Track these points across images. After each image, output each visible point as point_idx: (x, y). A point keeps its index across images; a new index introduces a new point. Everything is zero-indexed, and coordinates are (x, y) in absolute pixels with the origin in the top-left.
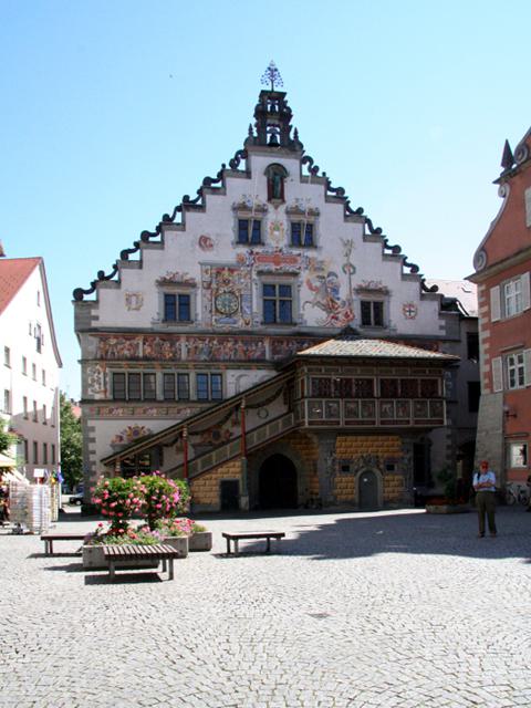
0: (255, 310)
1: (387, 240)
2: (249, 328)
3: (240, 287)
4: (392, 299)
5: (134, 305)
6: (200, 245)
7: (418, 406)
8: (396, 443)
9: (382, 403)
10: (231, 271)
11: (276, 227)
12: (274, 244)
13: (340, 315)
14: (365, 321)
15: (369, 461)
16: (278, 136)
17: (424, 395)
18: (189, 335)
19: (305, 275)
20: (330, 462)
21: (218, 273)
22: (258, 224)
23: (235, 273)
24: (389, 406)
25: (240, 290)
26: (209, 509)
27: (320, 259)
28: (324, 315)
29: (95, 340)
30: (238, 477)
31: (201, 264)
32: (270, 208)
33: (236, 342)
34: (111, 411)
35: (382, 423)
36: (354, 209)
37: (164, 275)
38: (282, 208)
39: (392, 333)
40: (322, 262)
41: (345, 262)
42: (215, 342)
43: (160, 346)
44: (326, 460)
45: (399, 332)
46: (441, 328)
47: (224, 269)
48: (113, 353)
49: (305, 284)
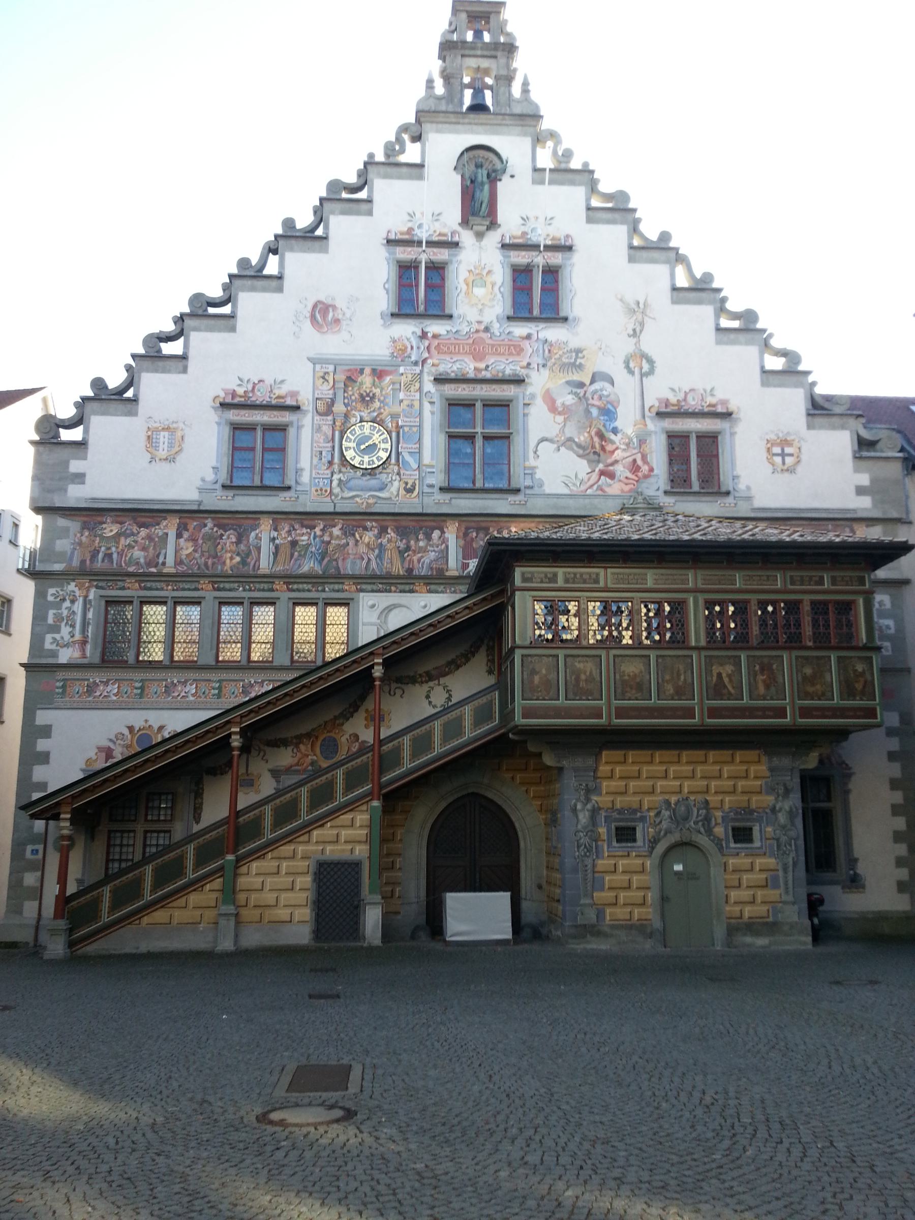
0: (427, 459)
1: (724, 300)
3: (396, 409)
4: (740, 428)
5: (162, 453)
6: (313, 317)
8: (753, 768)
9: (710, 660)
10: (378, 374)
11: (479, 277)
15: (686, 819)
16: (488, 94)
17: (822, 641)
18: (278, 516)
20: (584, 818)
21: (350, 380)
22: (437, 270)
23: (388, 379)
24: (729, 669)
25: (394, 416)
27: (574, 343)
28: (582, 467)
29: (72, 525)
30: (361, 851)
31: (314, 361)
32: (466, 237)
33: (383, 531)
34: (91, 689)
35: (714, 712)
36: (653, 236)
37: (233, 385)
38: (493, 239)
39: (743, 510)
40: (578, 351)
42: (336, 531)
43: (214, 540)
44: (574, 810)
45: (757, 503)
46: (860, 491)
47: (361, 371)
48: (109, 556)
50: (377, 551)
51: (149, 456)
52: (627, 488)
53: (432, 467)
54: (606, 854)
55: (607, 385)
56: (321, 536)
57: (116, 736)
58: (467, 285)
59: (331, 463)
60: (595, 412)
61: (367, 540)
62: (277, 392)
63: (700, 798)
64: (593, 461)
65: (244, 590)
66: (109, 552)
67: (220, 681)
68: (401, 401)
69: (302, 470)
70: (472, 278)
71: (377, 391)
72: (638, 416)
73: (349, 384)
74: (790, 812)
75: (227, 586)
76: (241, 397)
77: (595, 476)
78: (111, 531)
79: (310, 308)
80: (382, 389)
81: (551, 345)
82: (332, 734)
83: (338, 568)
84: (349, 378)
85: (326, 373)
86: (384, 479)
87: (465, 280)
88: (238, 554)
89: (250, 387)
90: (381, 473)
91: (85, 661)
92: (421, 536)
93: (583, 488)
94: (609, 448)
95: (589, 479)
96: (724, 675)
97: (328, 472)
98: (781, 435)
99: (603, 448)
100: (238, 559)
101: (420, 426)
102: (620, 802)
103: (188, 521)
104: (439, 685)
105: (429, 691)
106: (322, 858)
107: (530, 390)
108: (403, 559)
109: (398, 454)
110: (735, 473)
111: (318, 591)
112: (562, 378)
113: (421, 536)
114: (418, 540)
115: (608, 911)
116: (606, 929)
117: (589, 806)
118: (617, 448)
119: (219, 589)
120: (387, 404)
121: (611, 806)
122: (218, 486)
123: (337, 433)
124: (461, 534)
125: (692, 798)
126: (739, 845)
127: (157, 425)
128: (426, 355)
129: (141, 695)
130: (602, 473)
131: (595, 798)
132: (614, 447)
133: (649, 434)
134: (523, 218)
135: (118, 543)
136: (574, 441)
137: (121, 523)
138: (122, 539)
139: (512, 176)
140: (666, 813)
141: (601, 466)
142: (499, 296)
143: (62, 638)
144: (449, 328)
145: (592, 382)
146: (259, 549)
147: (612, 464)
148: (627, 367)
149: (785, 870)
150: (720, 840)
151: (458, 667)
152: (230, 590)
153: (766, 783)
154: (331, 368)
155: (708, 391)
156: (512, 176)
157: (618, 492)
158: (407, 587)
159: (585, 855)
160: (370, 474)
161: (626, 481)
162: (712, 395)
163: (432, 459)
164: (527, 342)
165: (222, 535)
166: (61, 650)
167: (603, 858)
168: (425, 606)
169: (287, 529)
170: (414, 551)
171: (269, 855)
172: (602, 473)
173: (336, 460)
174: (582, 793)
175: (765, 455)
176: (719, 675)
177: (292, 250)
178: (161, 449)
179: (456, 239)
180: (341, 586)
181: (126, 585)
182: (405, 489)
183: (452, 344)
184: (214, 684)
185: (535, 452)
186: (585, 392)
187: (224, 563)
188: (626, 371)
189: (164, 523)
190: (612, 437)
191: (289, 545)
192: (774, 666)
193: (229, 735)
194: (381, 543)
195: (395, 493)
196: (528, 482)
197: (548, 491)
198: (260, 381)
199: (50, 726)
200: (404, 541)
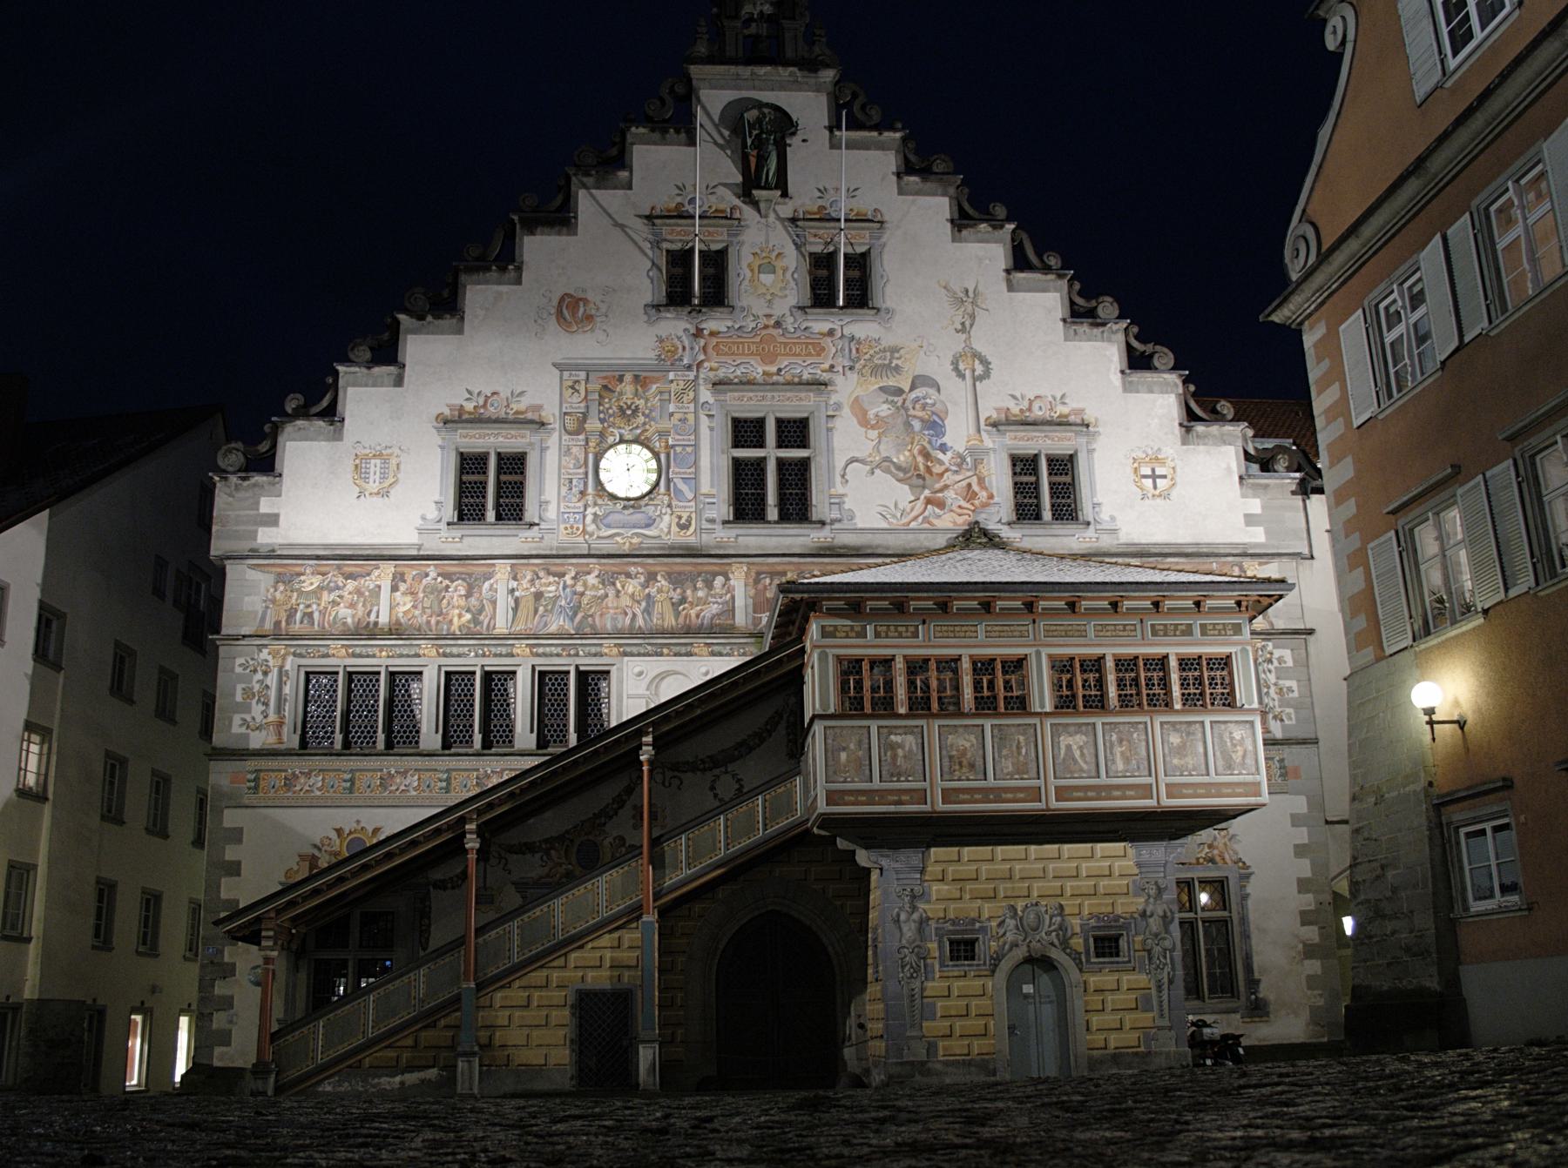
0: (705, 487)
2: (689, 538)
3: (665, 425)
4: (1100, 445)
6: (560, 314)
7: (1175, 739)
10: (641, 381)
12: (759, 308)
13: (950, 495)
14: (1027, 511)
15: (1035, 929)
19: (846, 388)
20: (909, 931)
24: (1080, 739)
25: (663, 434)
26: (540, 1085)
27: (889, 340)
28: (903, 494)
33: (651, 577)
34: (289, 783)
39: (1106, 542)
40: (894, 350)
41: (960, 347)
42: (592, 579)
43: (438, 593)
47: (621, 379)
48: (310, 615)
49: (846, 411)
50: (644, 604)
51: (358, 489)
52: (960, 520)
53: (713, 496)
54: (937, 975)
55: (932, 391)
56: (573, 586)
57: (322, 841)
58: (752, 270)
59: (583, 493)
60: (917, 425)
61: (630, 590)
62: (515, 407)
63: (1053, 902)
64: (917, 487)
65: (476, 656)
66: (309, 610)
67: (448, 771)
68: (671, 415)
69: (547, 502)
70: (758, 263)
71: (641, 403)
72: (972, 430)
73: (604, 394)
74: (1164, 917)
75: (455, 650)
76: (470, 413)
77: (920, 505)
78: (312, 584)
79: (555, 302)
80: (647, 400)
81: (859, 342)
82: (591, 837)
83: (593, 626)
84: (605, 387)
85: (577, 382)
86: (651, 514)
87: (749, 266)
88: (468, 611)
89: (481, 401)
90: (647, 505)
91: (283, 747)
92: (700, 584)
93: (905, 520)
94: (937, 469)
95: (912, 510)
96: (1075, 747)
97: (580, 504)
98: (1150, 452)
99: (928, 469)
100: (468, 616)
101: (696, 446)
102: (953, 910)
103: (406, 570)
104: (726, 772)
105: (714, 781)
106: (582, 986)
107: (834, 399)
108: (677, 614)
109: (669, 481)
110: (1095, 500)
111: (569, 655)
112: (875, 384)
113: (700, 584)
114: (695, 589)
115: (941, 1044)
116: (939, 1067)
117: (916, 916)
118: (947, 470)
119: (445, 655)
120: (653, 419)
121: (942, 915)
122: (443, 526)
123: (591, 457)
124: (751, 580)
125: (1044, 903)
126: (1101, 960)
127: (368, 451)
128: (702, 357)
129: (351, 790)
130: (929, 501)
131: (922, 906)
132: (943, 468)
133: (987, 451)
134: (820, 190)
135: (320, 599)
136: (892, 462)
137: (323, 574)
138: (325, 593)
139: (804, 141)
140: (1011, 923)
141: (927, 492)
142: (793, 284)
143: (254, 719)
144: (730, 324)
145: (912, 389)
146: (494, 603)
147: (941, 490)
148: (956, 369)
149: (1159, 988)
150: (1080, 953)
151: (751, 749)
152: (459, 656)
153: (1134, 882)
154: (582, 375)
155: (1058, 397)
156: (804, 141)
157: (951, 526)
158: (683, 650)
159: (912, 977)
160: (633, 507)
161: (960, 511)
162: (1064, 403)
163: (712, 486)
164: (829, 340)
165: (448, 587)
166: (252, 734)
167: (933, 979)
168: (707, 673)
169: (529, 577)
170: (691, 604)
171: (517, 984)
172: (929, 501)
173: (590, 490)
174: (907, 899)
175: (1133, 477)
176: (1069, 747)
177: (532, 233)
178: (371, 480)
179: (737, 215)
180: (598, 649)
181: (331, 652)
182: (678, 525)
183: (734, 343)
184: (440, 775)
185: (843, 476)
186: (904, 400)
187: (451, 621)
188: (954, 374)
189: (376, 573)
190: (940, 456)
191: (531, 598)
192: (1135, 735)
193: (463, 834)
194: (649, 595)
195: (666, 530)
196: (835, 515)
197: (860, 525)
198: (494, 394)
199: (242, 829)
200: (678, 591)
